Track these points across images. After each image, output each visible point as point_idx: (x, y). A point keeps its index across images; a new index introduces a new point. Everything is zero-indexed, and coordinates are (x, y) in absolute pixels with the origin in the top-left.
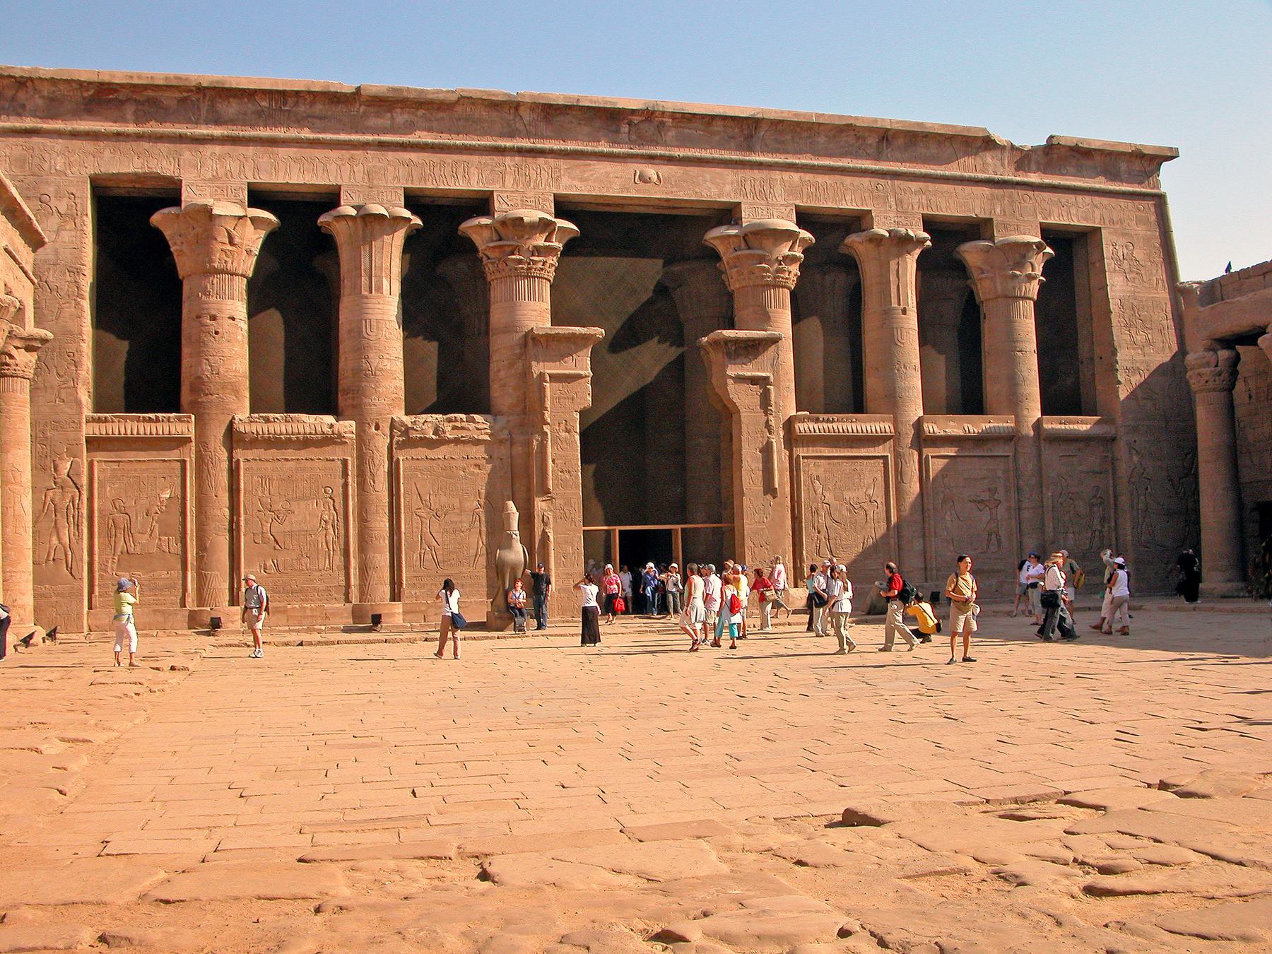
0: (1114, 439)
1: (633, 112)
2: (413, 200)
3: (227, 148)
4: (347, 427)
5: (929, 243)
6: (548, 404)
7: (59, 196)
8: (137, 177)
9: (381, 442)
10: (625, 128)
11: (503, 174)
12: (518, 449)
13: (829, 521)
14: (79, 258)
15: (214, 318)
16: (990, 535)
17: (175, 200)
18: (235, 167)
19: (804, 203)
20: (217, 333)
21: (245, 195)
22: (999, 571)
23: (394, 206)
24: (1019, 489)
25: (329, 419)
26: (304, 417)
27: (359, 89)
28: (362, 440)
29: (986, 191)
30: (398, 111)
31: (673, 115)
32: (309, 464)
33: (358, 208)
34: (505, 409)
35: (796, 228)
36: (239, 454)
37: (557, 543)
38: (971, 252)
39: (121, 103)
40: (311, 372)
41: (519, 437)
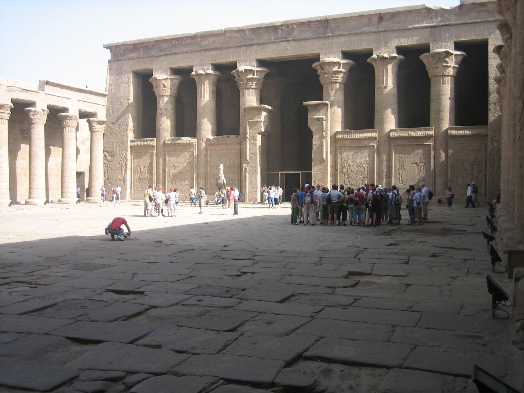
0: (487, 135)
1: (281, 25)
4: (194, 141)
5: (402, 57)
6: (248, 131)
8: (144, 70)
9: (203, 145)
10: (280, 32)
13: (349, 170)
14: (129, 96)
19: (345, 49)
23: (208, 69)
25: (189, 138)
27: (196, 34)
28: (199, 144)
29: (429, 30)
31: (295, 24)
37: (250, 178)
38: (423, 57)
40: (185, 125)
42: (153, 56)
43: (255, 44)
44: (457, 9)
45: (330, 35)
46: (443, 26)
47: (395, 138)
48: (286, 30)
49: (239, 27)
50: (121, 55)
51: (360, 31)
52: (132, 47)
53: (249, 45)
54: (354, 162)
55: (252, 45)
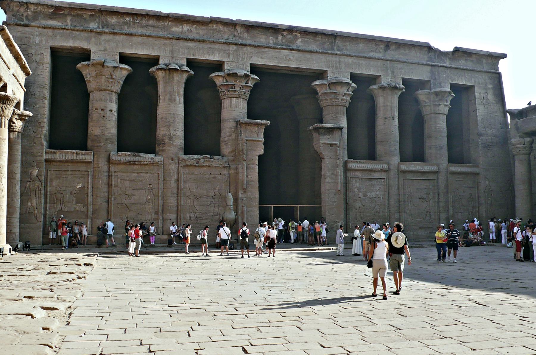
1: (284, 30)
2: (190, 63)
3: (111, 37)
5: (404, 90)
7: (36, 54)
10: (280, 37)
11: (229, 54)
12: (232, 172)
13: (360, 205)
15: (103, 110)
16: (427, 212)
17: (88, 58)
18: (113, 45)
20: (104, 117)
21: (118, 58)
22: (431, 228)
24: (439, 194)
26: (141, 154)
30: (185, 25)
32: (142, 175)
33: (167, 65)
34: (226, 154)
35: (350, 82)
36: (112, 168)
38: (422, 94)
39: (65, 15)
41: (232, 167)
42: (91, 31)
43: (250, 45)
44: (451, 54)
45: (339, 53)
46: (441, 66)
47: (404, 172)
48: (289, 36)
49: (232, 20)
50: (27, 18)
51: (368, 55)
52: (51, 10)
53: (241, 45)
54: (365, 195)
55: (245, 45)
